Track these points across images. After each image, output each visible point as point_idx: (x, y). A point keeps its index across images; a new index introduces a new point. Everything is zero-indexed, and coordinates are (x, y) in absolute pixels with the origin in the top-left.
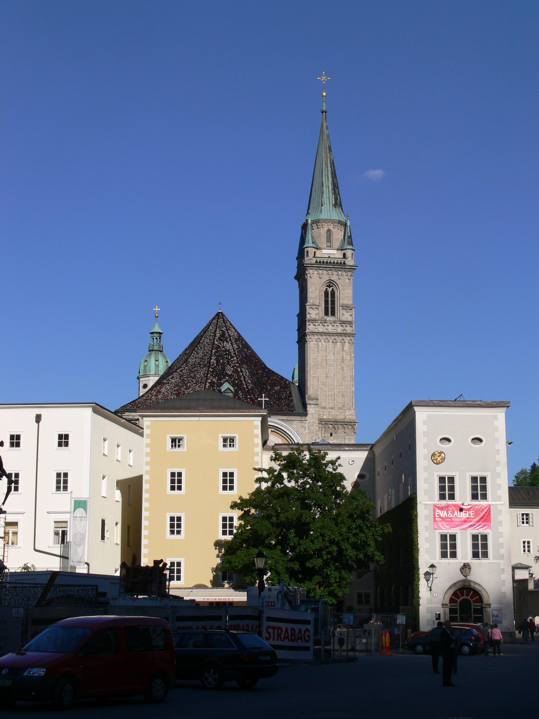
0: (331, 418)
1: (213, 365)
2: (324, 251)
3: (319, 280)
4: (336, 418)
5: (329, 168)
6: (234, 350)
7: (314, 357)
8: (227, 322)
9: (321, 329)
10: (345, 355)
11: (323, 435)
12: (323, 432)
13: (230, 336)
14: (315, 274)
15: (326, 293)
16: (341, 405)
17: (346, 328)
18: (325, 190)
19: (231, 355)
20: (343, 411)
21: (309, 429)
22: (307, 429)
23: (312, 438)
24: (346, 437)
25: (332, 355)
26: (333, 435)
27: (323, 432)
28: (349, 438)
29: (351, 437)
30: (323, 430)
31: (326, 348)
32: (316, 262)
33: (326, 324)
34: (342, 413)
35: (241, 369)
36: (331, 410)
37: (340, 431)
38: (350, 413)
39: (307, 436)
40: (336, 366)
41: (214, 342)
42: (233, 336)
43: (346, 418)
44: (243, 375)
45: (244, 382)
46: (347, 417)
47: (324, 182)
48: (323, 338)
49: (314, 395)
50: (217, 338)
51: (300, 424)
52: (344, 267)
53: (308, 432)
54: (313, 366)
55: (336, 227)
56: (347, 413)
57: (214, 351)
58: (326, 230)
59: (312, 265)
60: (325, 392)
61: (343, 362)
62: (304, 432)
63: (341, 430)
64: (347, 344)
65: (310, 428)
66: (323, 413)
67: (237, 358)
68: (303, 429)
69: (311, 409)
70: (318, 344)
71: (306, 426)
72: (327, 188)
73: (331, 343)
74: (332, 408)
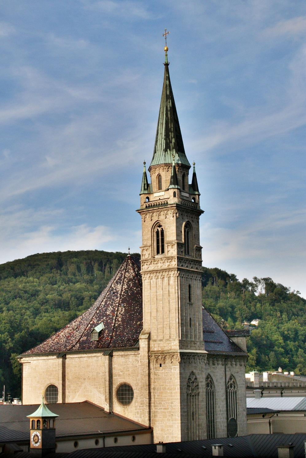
0: (160, 349)
1: (102, 306)
2: (155, 195)
3: (150, 222)
4: (164, 349)
5: (165, 116)
6: (122, 290)
7: (148, 294)
8: (129, 264)
9: (152, 267)
10: (171, 288)
11: (154, 366)
12: (154, 363)
13: (125, 277)
14: (148, 218)
15: (157, 233)
16: (169, 336)
17: (172, 263)
18: (159, 138)
19: (117, 296)
20: (168, 342)
21: (141, 362)
22: (140, 362)
23: (143, 370)
25: (160, 291)
26: (162, 366)
27: (154, 363)
28: (174, 367)
29: (176, 367)
30: (154, 362)
31: (156, 284)
32: (146, 207)
33: (155, 262)
34: (168, 344)
35: (118, 308)
36: (160, 343)
37: (167, 361)
38: (175, 343)
39: (140, 369)
41: (112, 285)
42: (128, 277)
43: (172, 349)
44: (117, 313)
45: (114, 320)
46: (172, 347)
47: (159, 130)
49: (148, 329)
50: (115, 281)
52: (166, 207)
53: (140, 364)
54: (147, 302)
55: (164, 170)
56: (172, 344)
57: (107, 294)
59: (142, 211)
62: (137, 365)
63: (168, 361)
64: (172, 279)
65: (142, 361)
66: (154, 345)
67: (120, 299)
68: (137, 362)
69: (143, 344)
71: (139, 359)
72: (161, 135)
73: (159, 279)
74: (161, 340)
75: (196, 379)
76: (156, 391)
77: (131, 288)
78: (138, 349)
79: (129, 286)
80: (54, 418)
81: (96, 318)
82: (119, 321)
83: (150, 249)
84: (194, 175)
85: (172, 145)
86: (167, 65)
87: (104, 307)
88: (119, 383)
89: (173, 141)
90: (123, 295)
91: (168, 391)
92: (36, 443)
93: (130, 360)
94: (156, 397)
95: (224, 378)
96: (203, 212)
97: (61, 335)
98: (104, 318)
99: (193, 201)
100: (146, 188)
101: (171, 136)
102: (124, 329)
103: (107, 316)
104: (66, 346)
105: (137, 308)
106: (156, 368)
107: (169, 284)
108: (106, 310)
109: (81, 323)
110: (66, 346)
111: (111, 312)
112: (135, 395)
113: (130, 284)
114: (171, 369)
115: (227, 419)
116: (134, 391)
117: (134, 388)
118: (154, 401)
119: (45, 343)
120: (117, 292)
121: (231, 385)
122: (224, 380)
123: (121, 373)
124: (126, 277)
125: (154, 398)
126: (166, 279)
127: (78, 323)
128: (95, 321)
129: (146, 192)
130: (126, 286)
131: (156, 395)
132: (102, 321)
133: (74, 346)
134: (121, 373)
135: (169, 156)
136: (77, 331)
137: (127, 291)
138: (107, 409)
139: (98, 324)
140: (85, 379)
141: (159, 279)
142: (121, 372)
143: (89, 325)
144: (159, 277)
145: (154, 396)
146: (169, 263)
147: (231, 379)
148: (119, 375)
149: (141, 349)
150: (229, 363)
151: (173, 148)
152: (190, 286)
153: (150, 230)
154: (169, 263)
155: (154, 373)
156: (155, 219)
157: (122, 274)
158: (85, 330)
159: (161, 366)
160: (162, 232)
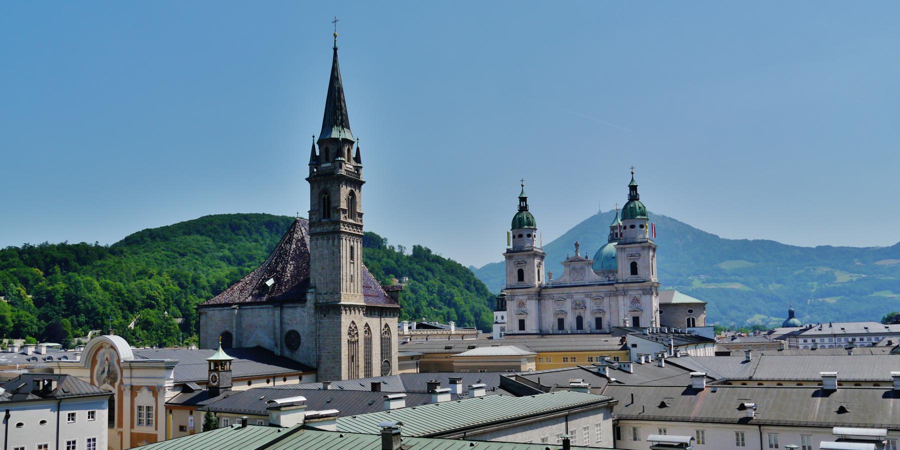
2: (324, 165)
15: (324, 199)
19: (286, 254)
20: (332, 295)
24: (335, 317)
34: (332, 297)
40: (329, 259)
41: (282, 244)
48: (320, 237)
50: (285, 242)
51: (301, 309)
56: (336, 297)
58: (324, 147)
60: (321, 281)
61: (334, 255)
64: (336, 240)
69: (309, 297)
70: (317, 243)
73: (325, 241)
74: (326, 294)
75: (356, 327)
76: (321, 337)
77: (300, 247)
78: (306, 301)
79: (297, 246)
80: (230, 361)
81: (268, 274)
82: (287, 276)
83: (318, 214)
84: (358, 149)
85: (339, 122)
86: (335, 49)
87: (274, 264)
88: (287, 331)
89: (340, 118)
90: (292, 254)
91: (332, 338)
92: (214, 382)
93: (298, 311)
94: (321, 342)
95: (379, 327)
96: (364, 182)
97: (235, 288)
98: (275, 274)
99: (356, 172)
100: (314, 158)
101: (337, 114)
102: (292, 283)
103: (277, 272)
104: (239, 298)
105: (304, 265)
106: (321, 318)
107: (334, 245)
108: (276, 267)
109: (253, 278)
110: (239, 298)
111: (281, 269)
112: (302, 341)
113: (298, 244)
114: (334, 318)
115: (382, 361)
116: (302, 338)
117: (301, 334)
118: (319, 346)
119: (220, 295)
120: (286, 251)
121: (386, 332)
122: (379, 329)
123: (290, 322)
124: (295, 238)
125: (319, 343)
126: (331, 240)
127: (251, 278)
128: (266, 277)
129: (315, 163)
130: (294, 246)
131: (321, 341)
132: (273, 277)
133: (247, 298)
134: (290, 322)
135: (336, 131)
136: (249, 285)
137: (296, 250)
138: (277, 352)
139: (269, 279)
140: (257, 327)
141: (325, 241)
142: (290, 321)
143: (261, 280)
144: (325, 238)
145: (319, 341)
146: (334, 227)
147: (385, 327)
148: (288, 324)
149: (308, 302)
150: (384, 314)
151: (340, 124)
152: (352, 248)
153: (318, 197)
154: (334, 227)
155: (319, 322)
156: (322, 187)
157: (291, 235)
158: (257, 284)
159: (325, 316)
160: (329, 198)
